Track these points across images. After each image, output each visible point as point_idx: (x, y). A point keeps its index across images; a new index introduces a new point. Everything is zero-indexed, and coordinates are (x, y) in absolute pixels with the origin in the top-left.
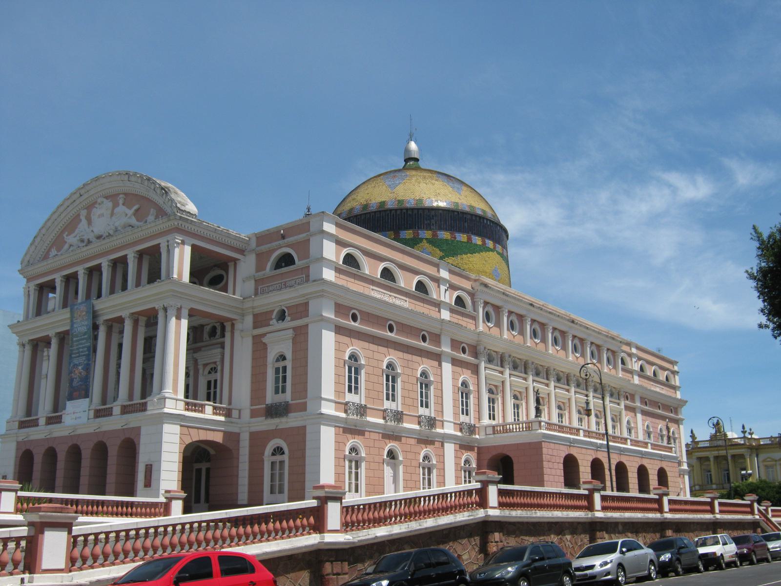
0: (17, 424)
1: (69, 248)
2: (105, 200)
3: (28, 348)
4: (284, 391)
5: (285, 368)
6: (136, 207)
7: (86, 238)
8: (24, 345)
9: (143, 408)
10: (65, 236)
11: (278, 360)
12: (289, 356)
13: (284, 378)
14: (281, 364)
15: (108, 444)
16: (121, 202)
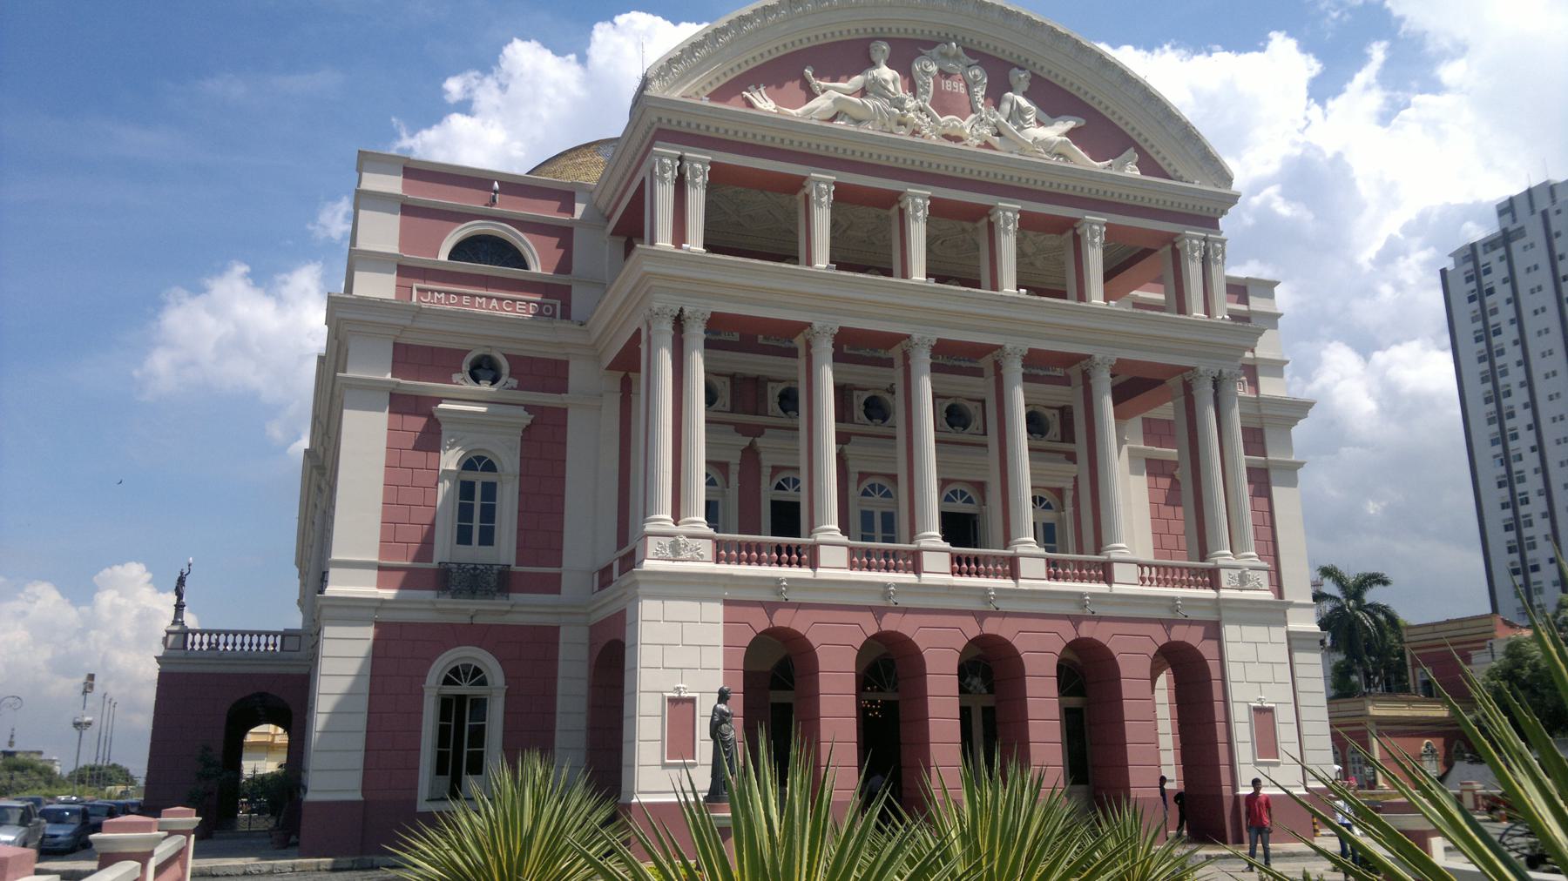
0: (707, 548)
2: (966, 59)
8: (679, 322)
10: (808, 72)
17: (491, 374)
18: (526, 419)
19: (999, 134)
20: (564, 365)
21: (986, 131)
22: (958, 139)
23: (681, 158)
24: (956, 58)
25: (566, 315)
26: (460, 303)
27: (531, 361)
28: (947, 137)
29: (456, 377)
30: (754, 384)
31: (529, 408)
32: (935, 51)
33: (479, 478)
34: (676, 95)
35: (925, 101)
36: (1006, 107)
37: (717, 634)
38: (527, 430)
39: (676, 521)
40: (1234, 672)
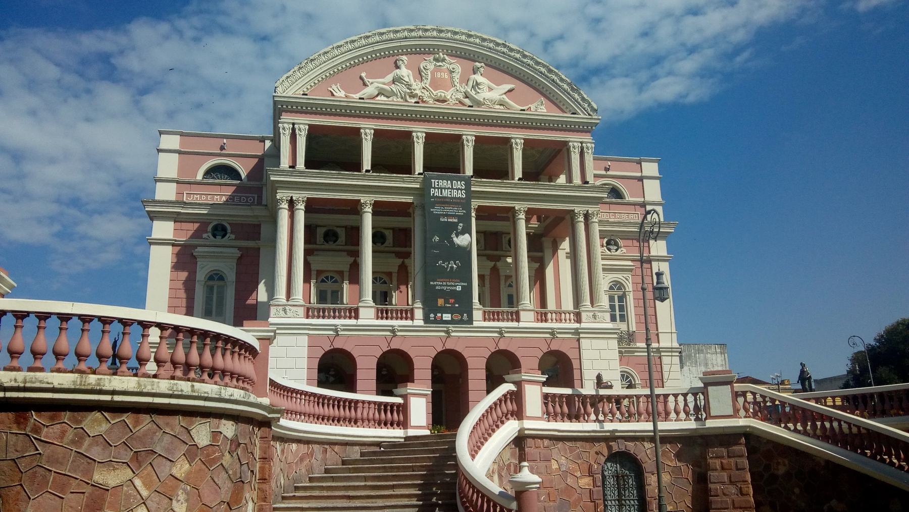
0: (301, 311)
1: (377, 96)
3: (301, 206)
4: (623, 318)
5: (622, 298)
6: (512, 86)
7: (418, 92)
8: (291, 203)
9: (578, 318)
10: (363, 75)
11: (611, 288)
12: (629, 287)
13: (622, 308)
14: (617, 294)
15: (518, 354)
16: (482, 69)
17: (223, 233)
18: (237, 253)
19: (467, 97)
20: (259, 226)
21: (460, 96)
22: (444, 101)
23: (293, 124)
24: (444, 60)
25: (260, 203)
26: (207, 200)
27: (242, 225)
28: (438, 101)
29: (205, 236)
30: (330, 232)
31: (240, 248)
32: (432, 58)
33: (216, 284)
34: (290, 94)
35: (427, 84)
36: (471, 83)
37: (304, 352)
38: (240, 259)
39: (288, 300)
40: (586, 364)
